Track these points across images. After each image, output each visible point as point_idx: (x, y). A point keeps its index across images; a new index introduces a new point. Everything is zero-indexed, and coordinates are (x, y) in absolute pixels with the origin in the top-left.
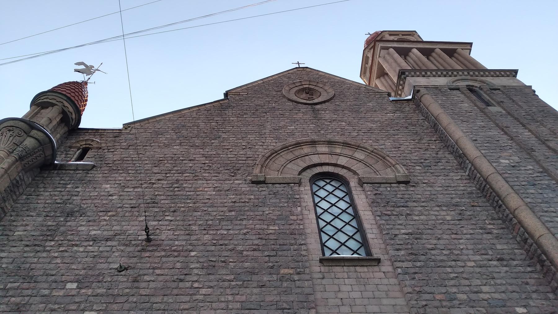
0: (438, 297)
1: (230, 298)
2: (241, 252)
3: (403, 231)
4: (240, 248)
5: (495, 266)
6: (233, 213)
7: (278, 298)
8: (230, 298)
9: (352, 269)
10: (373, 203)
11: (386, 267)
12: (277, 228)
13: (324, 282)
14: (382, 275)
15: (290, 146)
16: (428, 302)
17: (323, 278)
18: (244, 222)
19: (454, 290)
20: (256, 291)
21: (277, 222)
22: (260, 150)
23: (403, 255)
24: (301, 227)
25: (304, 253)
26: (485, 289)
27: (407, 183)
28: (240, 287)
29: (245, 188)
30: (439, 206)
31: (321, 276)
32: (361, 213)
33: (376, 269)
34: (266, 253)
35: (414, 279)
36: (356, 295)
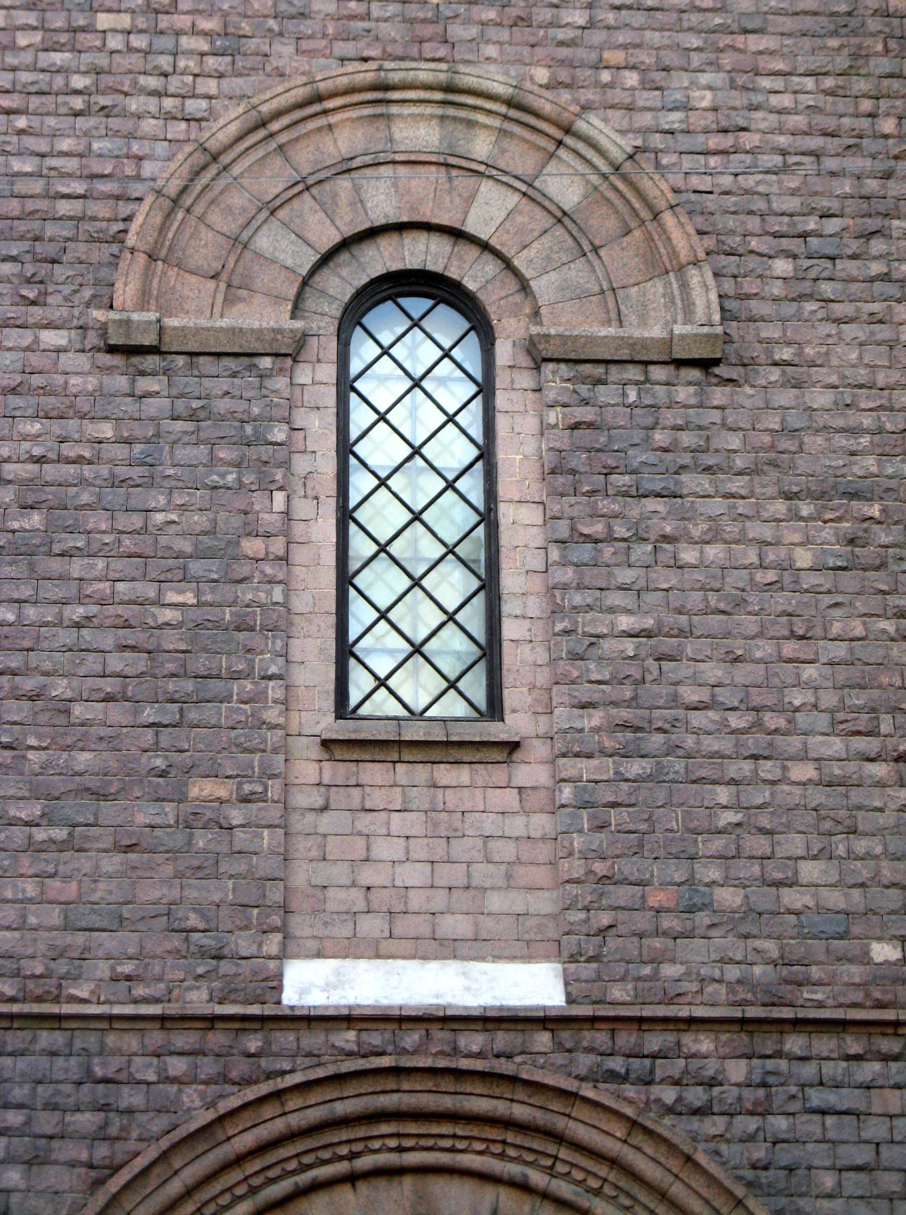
0: (656, 898)
1: (30, 889)
2: (64, 708)
3: (625, 622)
4: (60, 688)
5: (881, 784)
6: (36, 519)
7: (175, 893)
8: (30, 889)
9: (421, 773)
10: (556, 470)
11: (531, 772)
12: (189, 598)
13: (325, 822)
14: (510, 798)
15: (278, 114)
16: (623, 916)
17: (325, 808)
18: (77, 568)
19: (714, 873)
20: (112, 863)
21: (196, 567)
22: (149, 125)
23: (597, 730)
24: (278, 594)
25: (272, 715)
26: (810, 871)
27: (706, 364)
28: (62, 846)
29: (81, 374)
30: (789, 496)
31: (319, 802)
32: (506, 513)
33: (499, 774)
34: (149, 714)
35: (602, 827)
36: (413, 875)
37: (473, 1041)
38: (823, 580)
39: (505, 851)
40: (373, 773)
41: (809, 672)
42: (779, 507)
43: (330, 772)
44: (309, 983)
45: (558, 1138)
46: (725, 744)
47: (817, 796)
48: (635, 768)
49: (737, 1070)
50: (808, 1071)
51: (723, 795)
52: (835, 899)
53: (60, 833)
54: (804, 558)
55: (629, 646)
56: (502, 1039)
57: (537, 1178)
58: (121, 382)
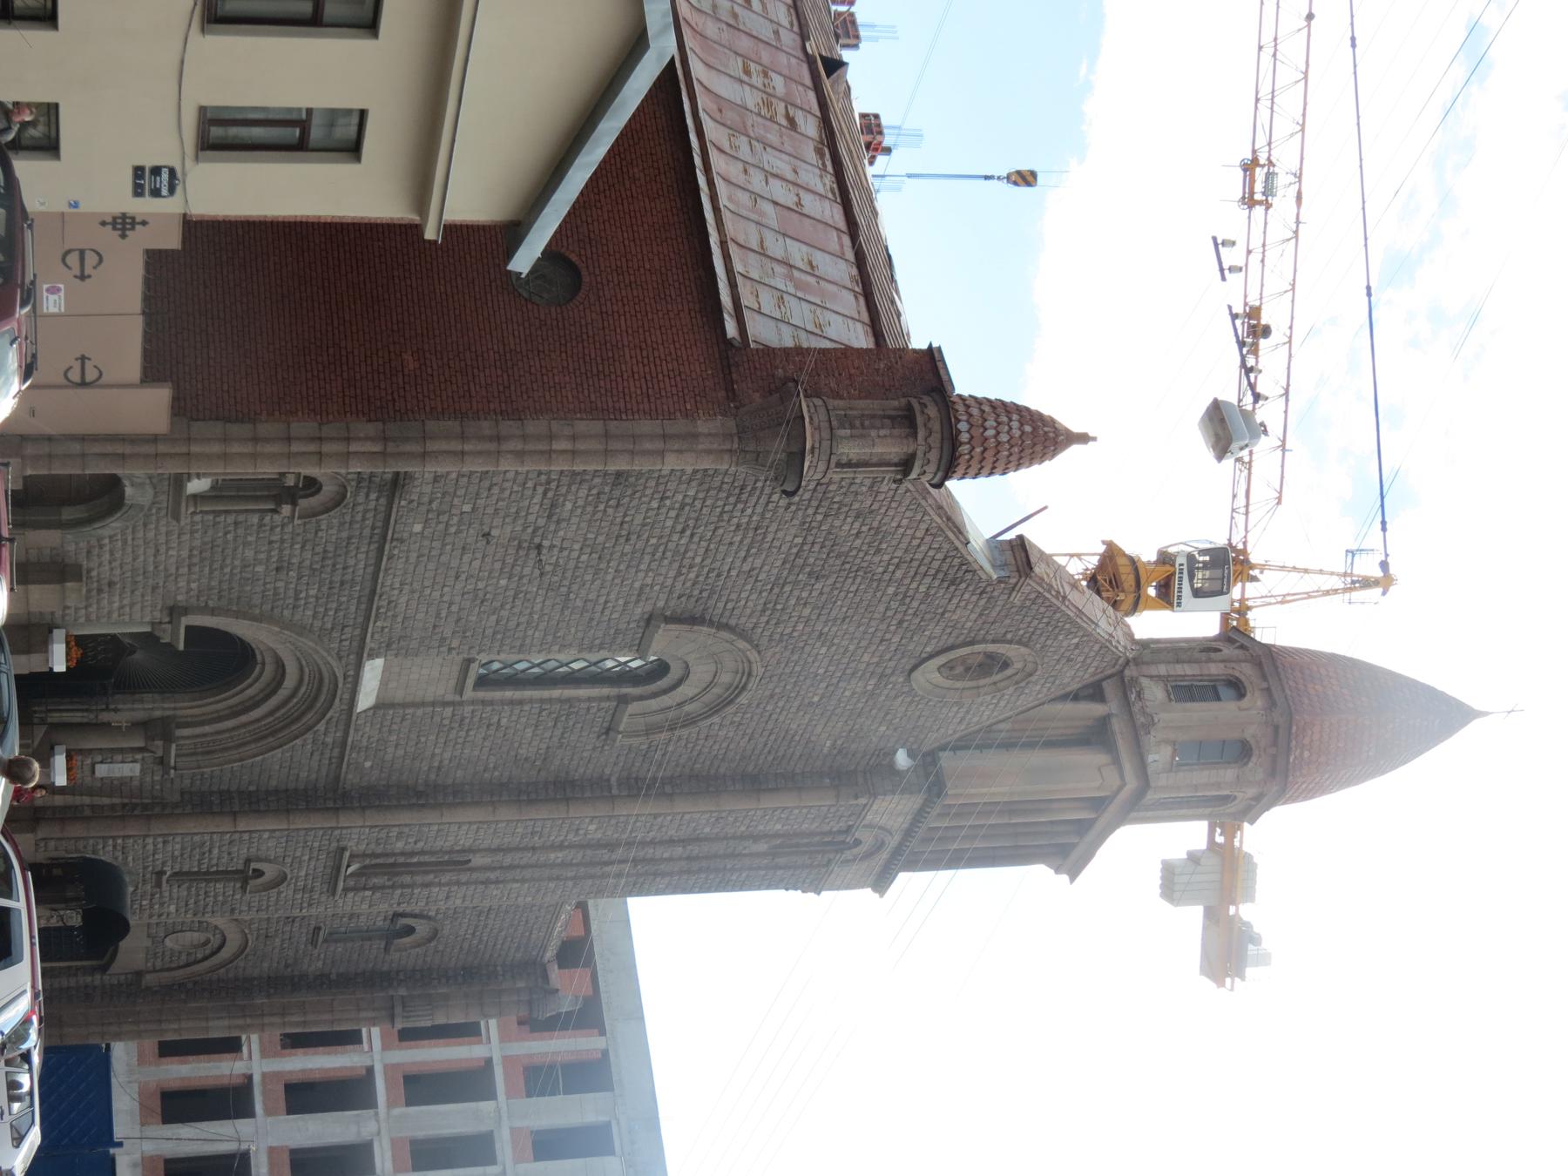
14: (441, 692)
37: (346, 696)
48: (446, 722)
49: (329, 740)
51: (433, 737)
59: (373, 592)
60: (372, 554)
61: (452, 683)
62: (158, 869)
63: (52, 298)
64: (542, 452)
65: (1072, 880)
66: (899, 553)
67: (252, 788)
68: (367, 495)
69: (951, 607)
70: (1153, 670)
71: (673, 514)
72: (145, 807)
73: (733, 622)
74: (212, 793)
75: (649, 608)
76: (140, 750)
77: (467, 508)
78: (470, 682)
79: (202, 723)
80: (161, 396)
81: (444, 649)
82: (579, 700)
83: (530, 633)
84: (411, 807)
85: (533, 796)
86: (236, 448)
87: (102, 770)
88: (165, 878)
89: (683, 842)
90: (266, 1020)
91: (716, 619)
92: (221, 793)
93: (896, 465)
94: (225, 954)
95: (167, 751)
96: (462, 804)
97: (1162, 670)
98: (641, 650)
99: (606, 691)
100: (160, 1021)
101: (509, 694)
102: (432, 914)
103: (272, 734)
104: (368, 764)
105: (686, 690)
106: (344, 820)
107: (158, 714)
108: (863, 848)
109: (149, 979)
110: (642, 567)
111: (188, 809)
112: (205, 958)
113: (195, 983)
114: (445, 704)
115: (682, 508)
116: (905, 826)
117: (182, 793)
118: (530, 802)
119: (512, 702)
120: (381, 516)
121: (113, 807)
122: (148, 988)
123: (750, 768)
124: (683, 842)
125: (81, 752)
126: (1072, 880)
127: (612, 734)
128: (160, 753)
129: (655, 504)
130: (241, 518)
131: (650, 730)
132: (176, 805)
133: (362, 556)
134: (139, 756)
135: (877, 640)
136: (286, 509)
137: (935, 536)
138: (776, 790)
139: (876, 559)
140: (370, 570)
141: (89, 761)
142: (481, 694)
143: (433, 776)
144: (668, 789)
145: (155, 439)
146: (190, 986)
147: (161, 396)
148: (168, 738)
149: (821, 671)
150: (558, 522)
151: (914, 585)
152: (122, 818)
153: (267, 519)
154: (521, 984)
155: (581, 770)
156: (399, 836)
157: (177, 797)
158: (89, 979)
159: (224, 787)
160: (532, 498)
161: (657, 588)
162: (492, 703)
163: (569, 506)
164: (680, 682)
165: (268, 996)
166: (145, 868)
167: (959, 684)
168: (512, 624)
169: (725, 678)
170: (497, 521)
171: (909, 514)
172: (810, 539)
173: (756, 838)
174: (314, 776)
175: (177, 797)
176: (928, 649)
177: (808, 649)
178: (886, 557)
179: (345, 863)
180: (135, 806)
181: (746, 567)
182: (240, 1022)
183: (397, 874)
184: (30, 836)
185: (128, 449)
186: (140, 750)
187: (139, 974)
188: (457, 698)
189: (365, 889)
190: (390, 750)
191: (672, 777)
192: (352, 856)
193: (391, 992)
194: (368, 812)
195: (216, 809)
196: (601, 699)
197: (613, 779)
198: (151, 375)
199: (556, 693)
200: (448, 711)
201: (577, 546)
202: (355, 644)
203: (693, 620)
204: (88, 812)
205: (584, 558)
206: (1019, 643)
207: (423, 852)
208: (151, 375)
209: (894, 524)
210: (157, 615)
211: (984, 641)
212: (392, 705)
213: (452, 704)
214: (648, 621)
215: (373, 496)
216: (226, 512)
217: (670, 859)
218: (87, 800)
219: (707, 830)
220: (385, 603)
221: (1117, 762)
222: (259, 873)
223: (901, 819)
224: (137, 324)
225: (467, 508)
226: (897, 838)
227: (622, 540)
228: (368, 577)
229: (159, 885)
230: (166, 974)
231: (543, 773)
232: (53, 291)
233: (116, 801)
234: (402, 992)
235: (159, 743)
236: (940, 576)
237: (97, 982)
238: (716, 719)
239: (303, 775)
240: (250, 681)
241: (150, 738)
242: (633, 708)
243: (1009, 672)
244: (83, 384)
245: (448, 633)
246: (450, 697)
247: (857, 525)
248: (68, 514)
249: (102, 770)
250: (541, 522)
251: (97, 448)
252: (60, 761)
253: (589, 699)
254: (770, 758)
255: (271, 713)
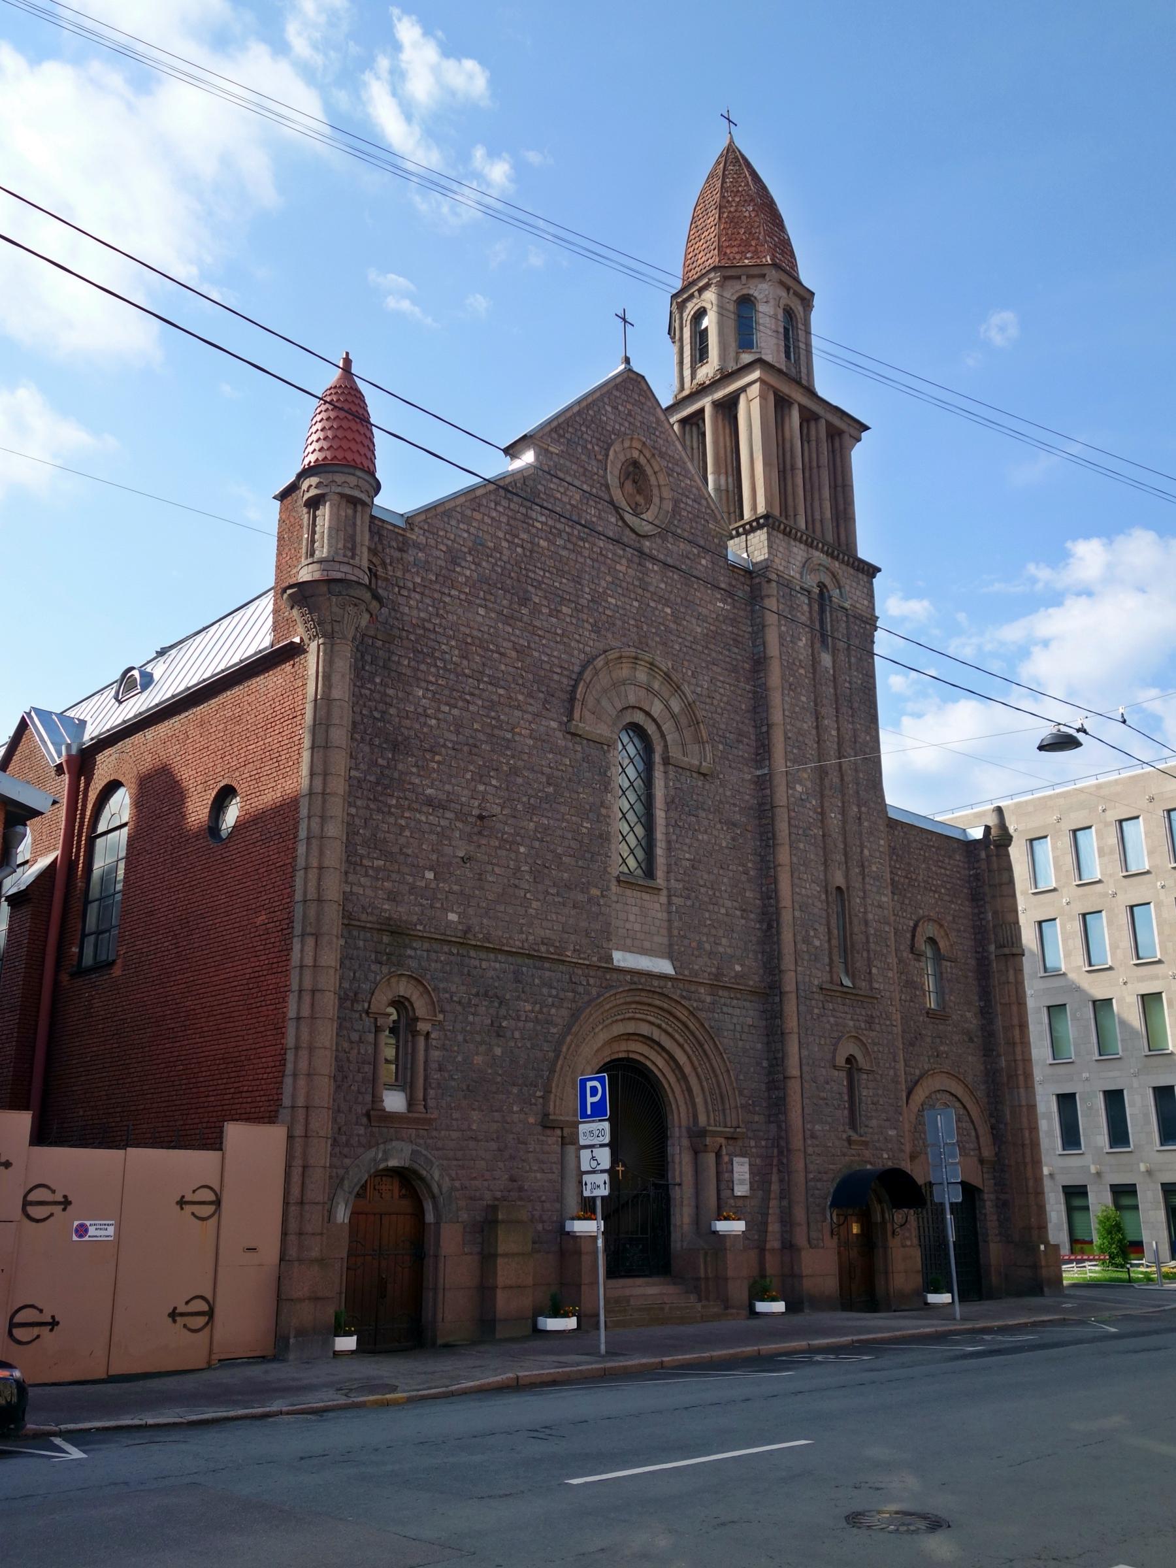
2: (559, 856)
3: (687, 856)
13: (619, 906)
14: (657, 906)
36: (637, 927)
37: (656, 983)
38: (726, 851)
39: (657, 923)
40: (628, 892)
41: (725, 880)
42: (719, 826)
43: (619, 890)
44: (622, 959)
45: (671, 1014)
46: (706, 899)
47: (726, 919)
49: (708, 999)
50: (723, 1000)
51: (707, 915)
52: (729, 950)
53: (561, 900)
54: (724, 844)
55: (688, 864)
56: (662, 983)
57: (664, 1025)
58: (570, 745)
59: (529, 956)
60: (483, 955)
61: (646, 896)
62: (846, 1144)
63: (92, 1231)
64: (324, 802)
65: (866, 428)
66: (501, 534)
67: (765, 1064)
68: (410, 957)
69: (565, 499)
70: (687, 379)
71: (446, 709)
72: (781, 1153)
73: (577, 669)
74: (770, 1098)
75: (559, 734)
76: (718, 1155)
77: (430, 875)
78: (651, 883)
79: (694, 1105)
80: (234, 1132)
81: (602, 902)
82: (666, 796)
83: (584, 830)
84: (779, 933)
85: (770, 835)
86: (303, 1065)
87: (741, 1190)
88: (855, 1137)
89: (818, 717)
90: (1019, 1057)
91: (572, 683)
92: (769, 1089)
93: (355, 512)
94: (959, 1091)
95: (715, 1134)
96: (776, 891)
97: (687, 373)
98: (604, 746)
99: (658, 774)
100: (1023, 1145)
101: (660, 851)
102: (911, 924)
103: (701, 1045)
104: (738, 968)
105: (657, 709)
106: (789, 984)
107: (685, 1142)
108: (827, 581)
109: (987, 1153)
110: (509, 736)
111: (782, 1117)
112: (965, 1107)
113: (991, 1115)
114: (670, 903)
115: (439, 701)
116: (802, 546)
117: (770, 1122)
118: (774, 837)
119: (669, 849)
120: (436, 946)
121: (781, 1181)
122: (996, 1154)
123: (747, 666)
124: (818, 717)
125: (719, 1208)
126: (866, 428)
127: (703, 771)
128: (723, 1141)
129: (433, 722)
130: (434, 1066)
131: (699, 741)
132: (779, 1127)
133: (484, 965)
134: (726, 1159)
135: (601, 559)
136: (422, 1027)
137: (480, 505)
138: (764, 644)
139: (506, 552)
140: (501, 957)
141: (732, 1201)
142: (660, 873)
143: (752, 916)
144: (764, 729)
145: (290, 1137)
146: (993, 1121)
147: (234, 1132)
148: (703, 1133)
149: (636, 604)
150: (451, 801)
151: (539, 525)
152: (789, 1173)
153: (434, 1043)
154: (983, 855)
155: (747, 797)
156: (807, 941)
157: (773, 1127)
158: (988, 1204)
159: (763, 1087)
160: (420, 821)
161: (533, 726)
162: (669, 865)
163: (429, 791)
164: (648, 714)
165: (999, 1056)
166: (844, 1155)
167: (656, 500)
168: (573, 844)
169: (642, 676)
170: (448, 850)
171: (453, 523)
172: (478, 601)
173: (815, 662)
174: (751, 1013)
175: (773, 1127)
176: (613, 520)
177: (608, 612)
178: (505, 544)
179: (840, 989)
180: (781, 1163)
181: (514, 654)
182: (1021, 1078)
183: (853, 945)
184: (803, 1253)
185: (298, 1162)
186: (718, 1155)
187: (982, 1161)
188: (665, 892)
189: (870, 973)
190: (721, 950)
191: (755, 727)
192: (832, 982)
193: (993, 957)
194: (783, 968)
195: (781, 1095)
196: (667, 779)
197: (759, 773)
198: (214, 1142)
199: (660, 815)
200: (675, 900)
201: (481, 788)
202: (592, 973)
203: (572, 700)
204: (785, 1203)
205: (494, 782)
206: (608, 450)
207: (828, 925)
208: (214, 1142)
209: (466, 535)
210: (551, 1140)
211: (605, 477)
212: (671, 945)
213: (669, 896)
214: (574, 735)
215: (409, 952)
216: (426, 1079)
217: (838, 729)
218: (773, 1203)
219: (804, 699)
220: (543, 948)
221: (743, 389)
222: (850, 1060)
223: (795, 550)
224: (132, 1152)
225: (430, 875)
226: (817, 553)
227: (475, 750)
228: (510, 959)
229: (866, 1144)
230: (982, 1140)
231: (749, 828)
232: (82, 1230)
233: (775, 1178)
234: (992, 948)
235: (708, 1140)
236: (529, 504)
237: (992, 1197)
238: (685, 688)
239: (749, 1021)
240: (648, 1064)
241: (705, 1148)
242: (675, 753)
243: (643, 461)
244: (217, 1203)
245: (581, 897)
246: (663, 899)
247: (467, 565)
248: (430, 1218)
249: (741, 1190)
250: (449, 815)
251: (296, 1191)
252: (722, 1226)
253: (666, 787)
254: (736, 650)
255: (681, 1046)
